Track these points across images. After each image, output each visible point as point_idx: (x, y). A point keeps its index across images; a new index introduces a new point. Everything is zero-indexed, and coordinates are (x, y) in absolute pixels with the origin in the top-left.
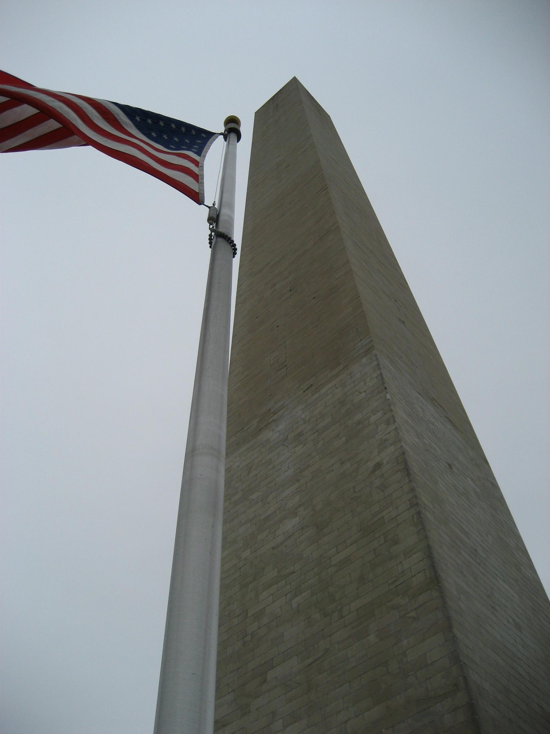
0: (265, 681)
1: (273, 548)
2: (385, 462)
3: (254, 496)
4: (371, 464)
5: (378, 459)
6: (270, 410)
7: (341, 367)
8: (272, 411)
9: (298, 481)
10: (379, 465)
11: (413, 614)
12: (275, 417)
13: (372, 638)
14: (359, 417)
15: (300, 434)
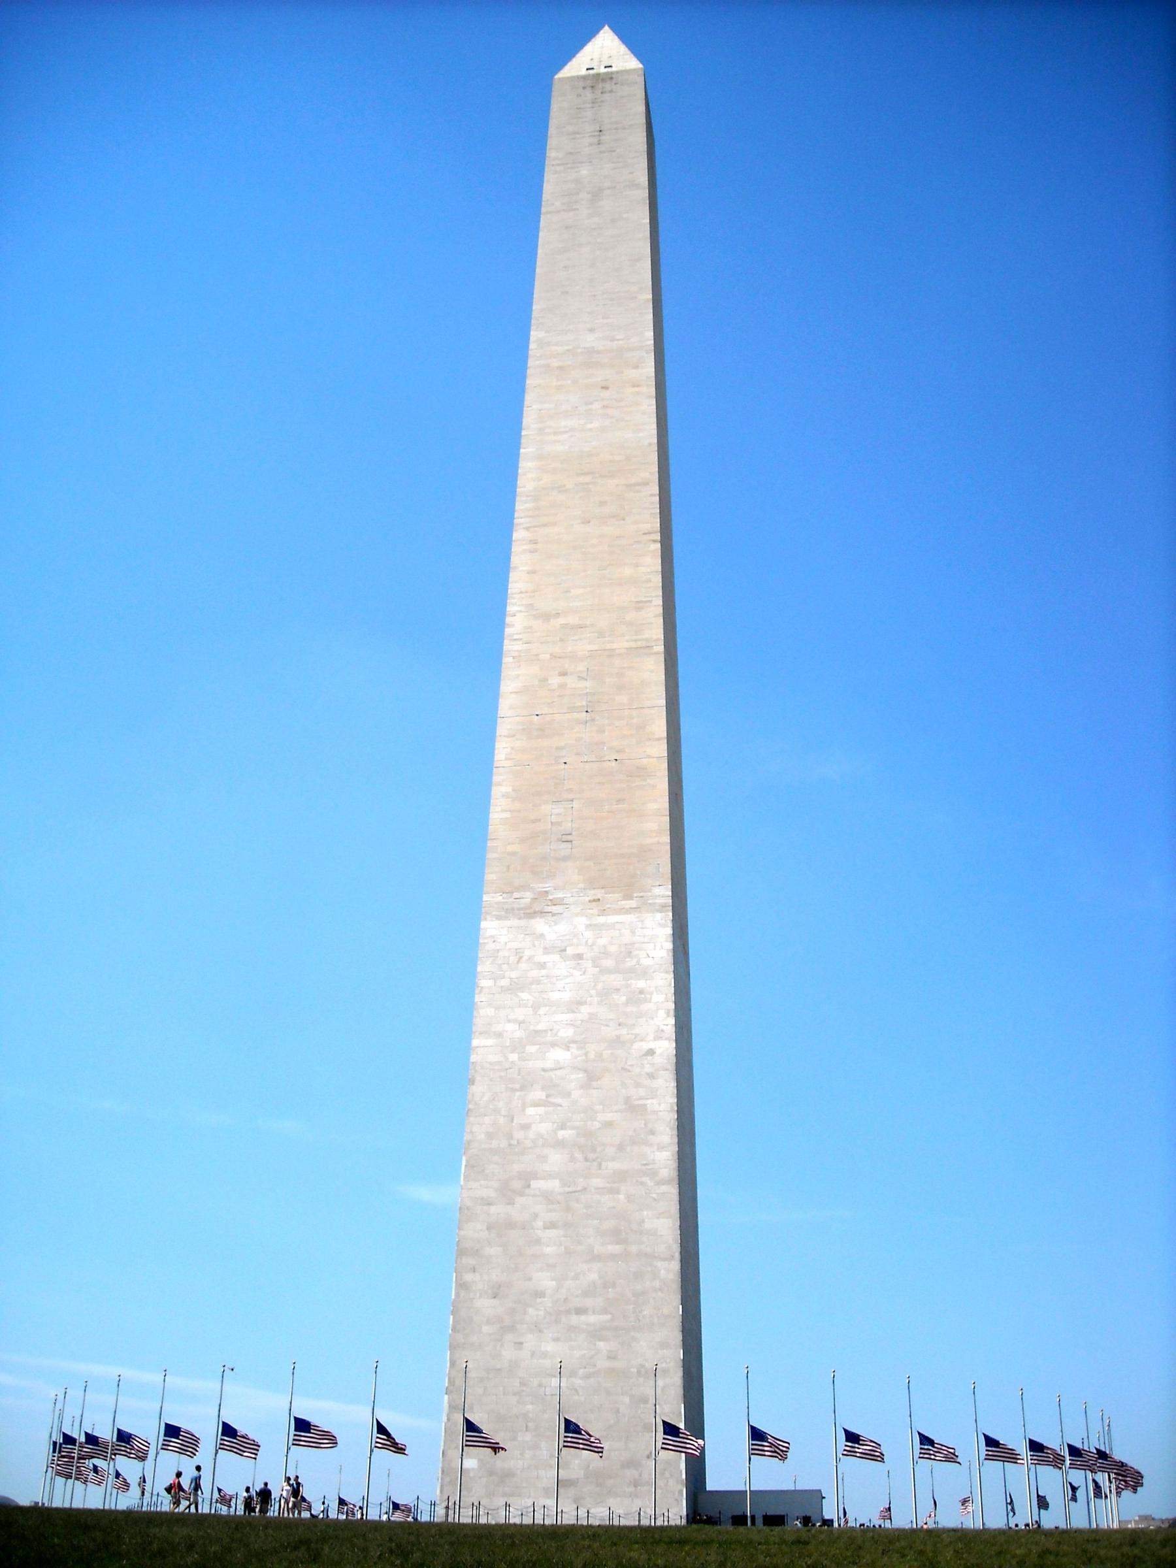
0: (529, 1186)
1: (544, 1070)
2: (658, 1052)
3: (524, 996)
4: (646, 1046)
5: (651, 1045)
6: (546, 892)
7: (632, 903)
8: (550, 897)
9: (573, 1012)
10: (651, 1052)
11: (654, 1196)
12: (554, 909)
13: (621, 1197)
14: (641, 984)
15: (579, 957)
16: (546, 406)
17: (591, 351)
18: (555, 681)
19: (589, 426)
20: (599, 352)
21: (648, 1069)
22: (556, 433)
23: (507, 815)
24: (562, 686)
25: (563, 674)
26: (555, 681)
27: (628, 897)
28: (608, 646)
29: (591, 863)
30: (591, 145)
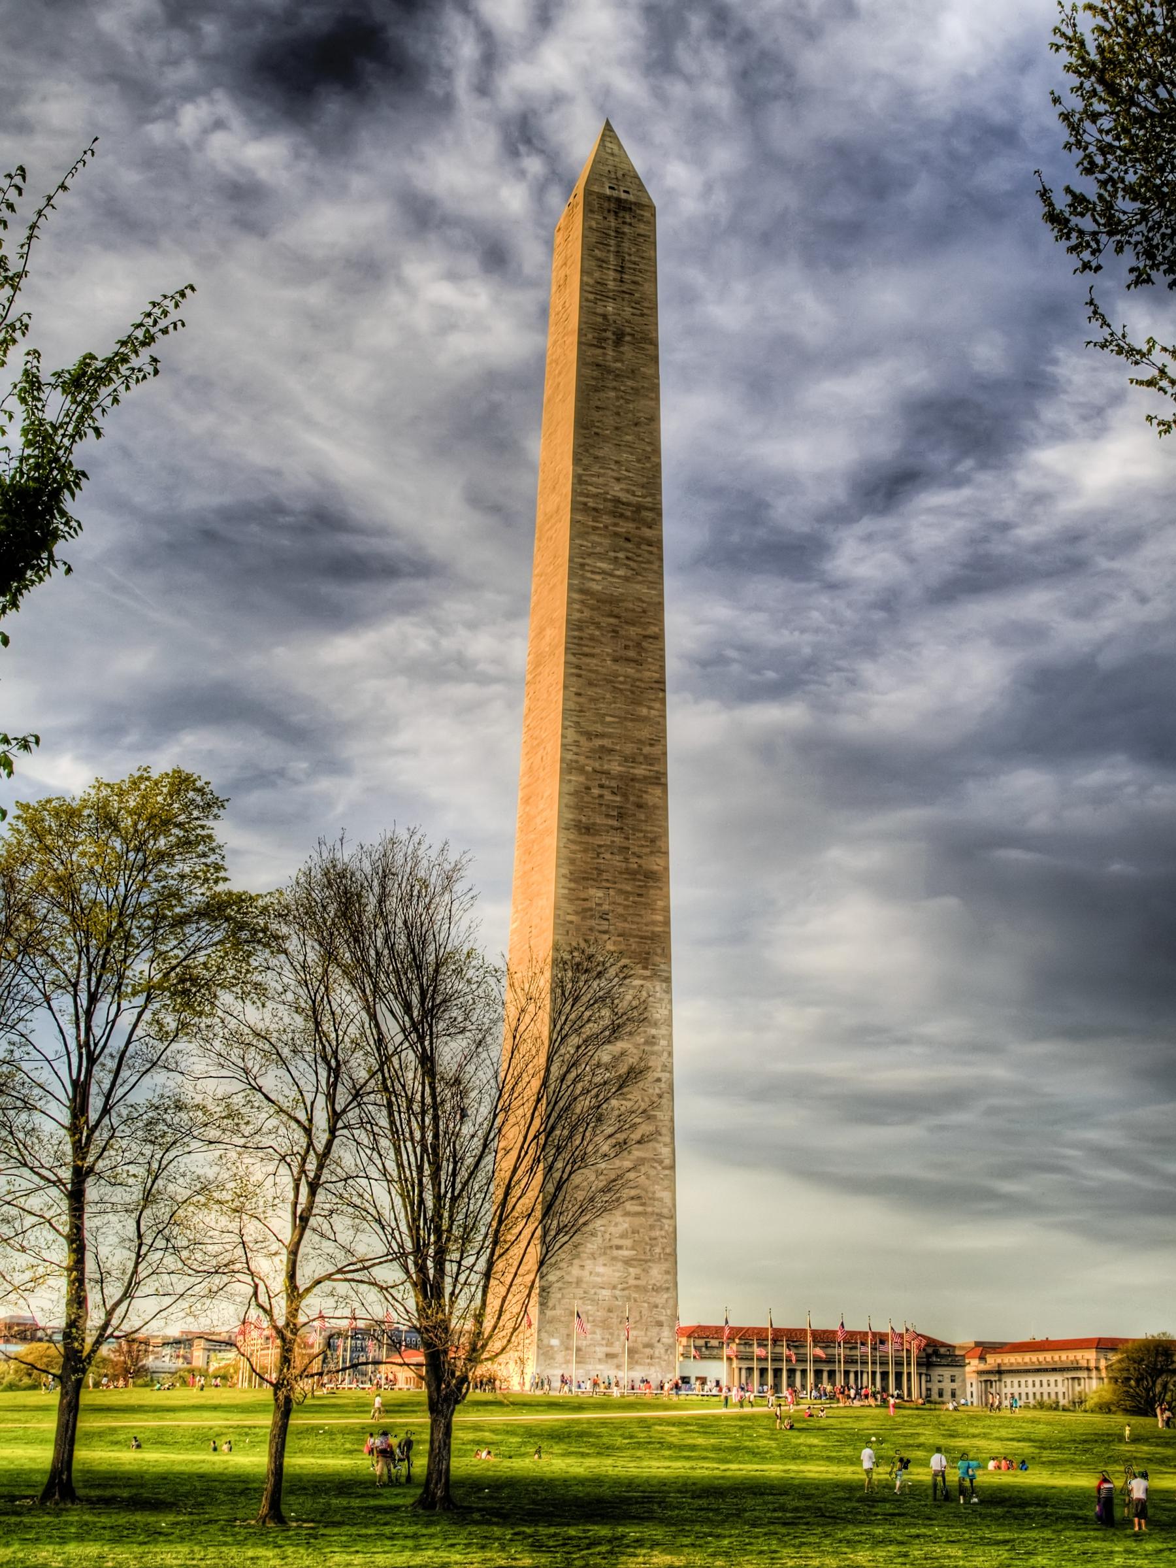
10: (659, 1080)
14: (653, 1031)
16: (585, 543)
17: (617, 501)
18: (596, 791)
19: (618, 573)
20: (623, 504)
21: (657, 1091)
22: (593, 572)
23: (566, 891)
24: (601, 796)
25: (601, 786)
26: (596, 791)
27: (645, 968)
28: (632, 771)
29: (621, 939)
30: (615, 280)
